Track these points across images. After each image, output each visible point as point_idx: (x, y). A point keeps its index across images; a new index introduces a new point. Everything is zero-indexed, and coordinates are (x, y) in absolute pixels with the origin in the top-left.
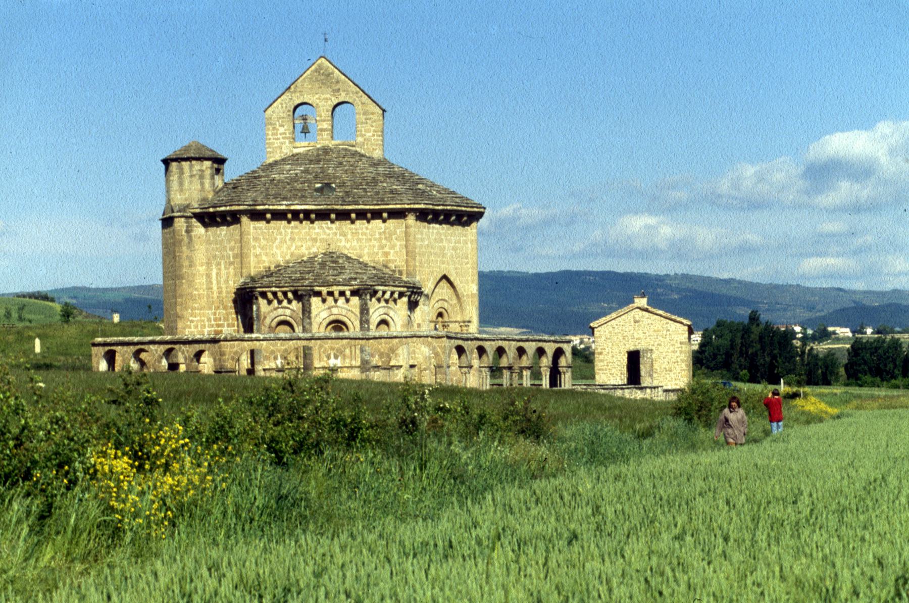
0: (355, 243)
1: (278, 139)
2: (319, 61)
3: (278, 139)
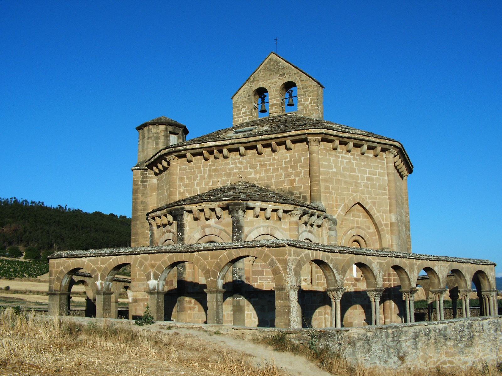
0: (263, 174)
1: (242, 117)
2: (270, 57)
3: (242, 117)
